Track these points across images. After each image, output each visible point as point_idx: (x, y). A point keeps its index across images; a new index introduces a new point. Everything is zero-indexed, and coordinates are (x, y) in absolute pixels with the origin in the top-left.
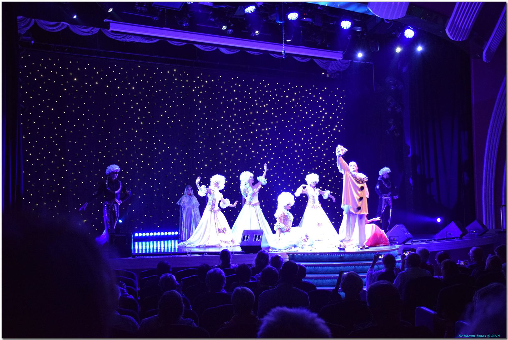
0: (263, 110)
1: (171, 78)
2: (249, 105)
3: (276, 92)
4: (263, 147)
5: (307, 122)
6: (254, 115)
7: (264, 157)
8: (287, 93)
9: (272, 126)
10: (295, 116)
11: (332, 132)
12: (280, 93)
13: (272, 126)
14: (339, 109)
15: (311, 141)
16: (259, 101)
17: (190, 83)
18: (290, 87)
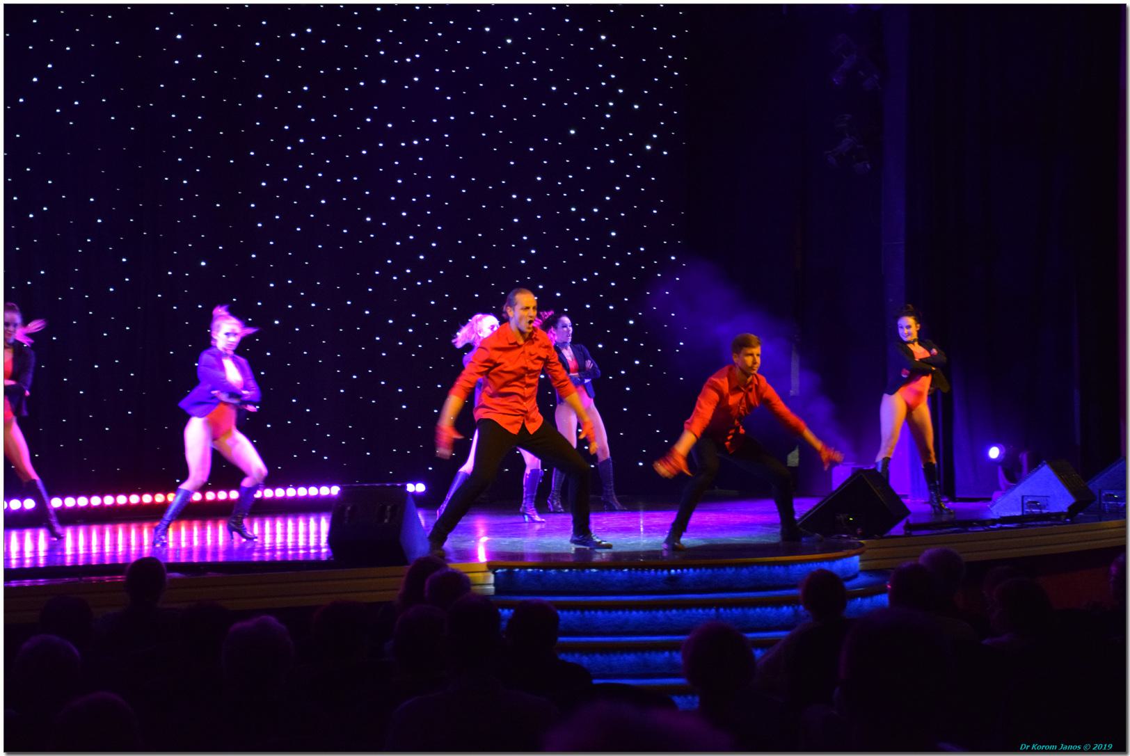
4: (403, 203)
7: (405, 241)
9: (435, 132)
11: (641, 155)
15: (568, 185)
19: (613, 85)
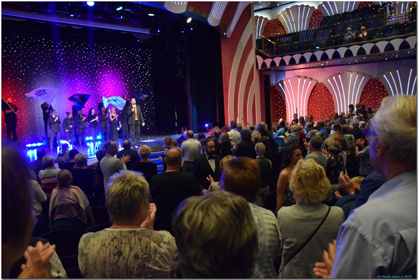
0: (104, 63)
1: (41, 45)
2: (94, 61)
3: (110, 53)
5: (130, 70)
6: (97, 67)
8: (117, 53)
10: (122, 67)
12: (113, 53)
13: (109, 73)
14: (149, 62)
16: (100, 58)
17: (54, 47)
18: (118, 49)
19: (140, 64)
